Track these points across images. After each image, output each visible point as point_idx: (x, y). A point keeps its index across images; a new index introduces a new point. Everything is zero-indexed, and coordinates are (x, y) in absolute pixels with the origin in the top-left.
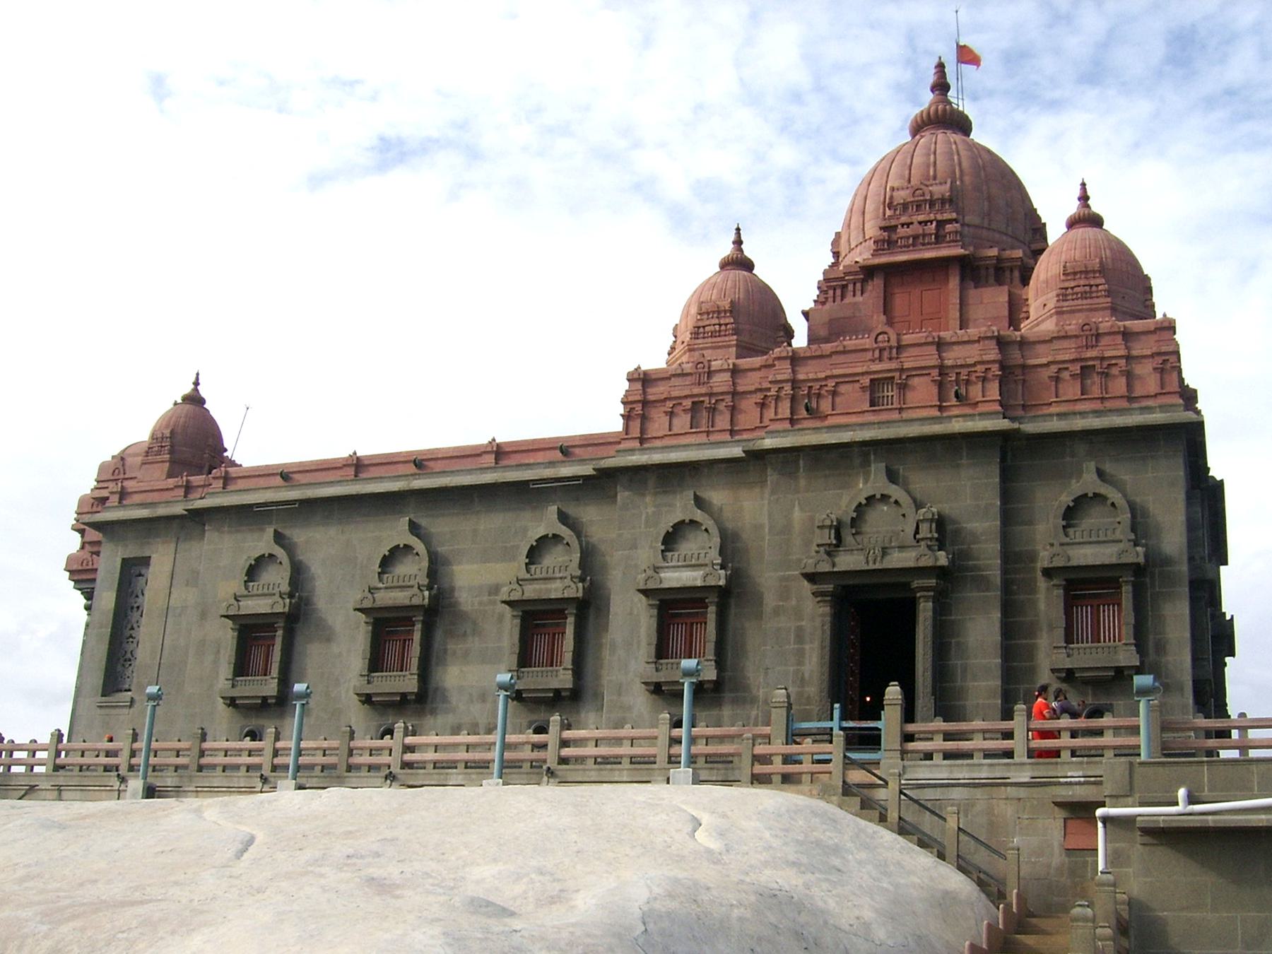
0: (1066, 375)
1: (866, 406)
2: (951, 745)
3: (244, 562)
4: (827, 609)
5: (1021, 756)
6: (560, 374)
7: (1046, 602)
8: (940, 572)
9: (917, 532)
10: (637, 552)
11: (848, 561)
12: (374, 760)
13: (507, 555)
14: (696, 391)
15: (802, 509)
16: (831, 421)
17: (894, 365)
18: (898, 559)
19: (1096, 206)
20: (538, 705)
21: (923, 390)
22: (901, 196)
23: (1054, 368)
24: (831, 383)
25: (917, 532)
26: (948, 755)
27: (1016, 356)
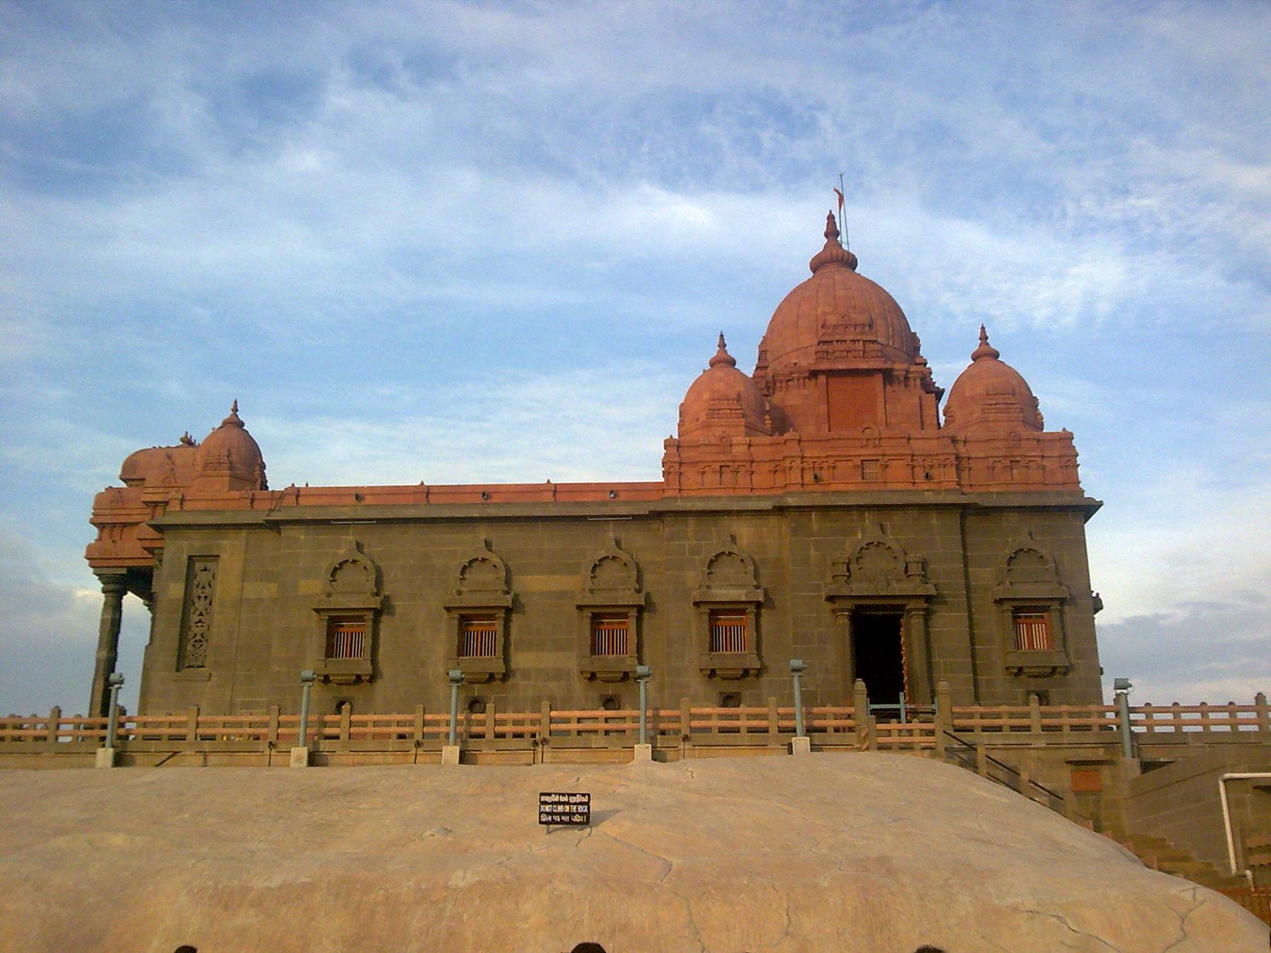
0: (999, 466)
1: (860, 480)
2: (987, 722)
3: (326, 565)
4: (844, 621)
5: (1036, 730)
6: (606, 432)
7: (992, 623)
8: (928, 599)
9: (906, 571)
10: (680, 574)
11: (859, 588)
12: (518, 729)
13: (572, 569)
14: (723, 457)
15: (816, 549)
16: (832, 488)
17: (878, 451)
18: (898, 588)
19: (993, 344)
20: (612, 689)
21: (898, 470)
22: (832, 320)
23: (991, 460)
24: (831, 461)
25: (906, 571)
26: (985, 729)
27: (962, 449)
